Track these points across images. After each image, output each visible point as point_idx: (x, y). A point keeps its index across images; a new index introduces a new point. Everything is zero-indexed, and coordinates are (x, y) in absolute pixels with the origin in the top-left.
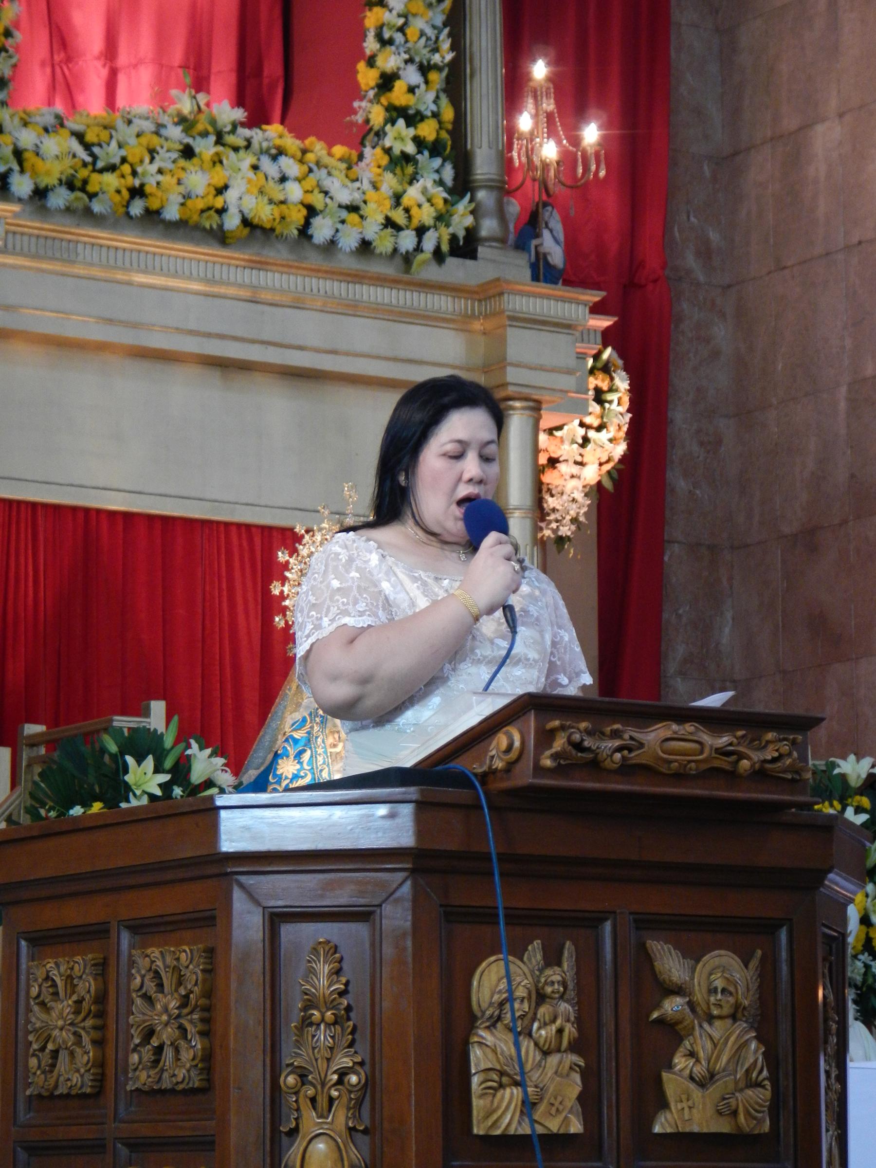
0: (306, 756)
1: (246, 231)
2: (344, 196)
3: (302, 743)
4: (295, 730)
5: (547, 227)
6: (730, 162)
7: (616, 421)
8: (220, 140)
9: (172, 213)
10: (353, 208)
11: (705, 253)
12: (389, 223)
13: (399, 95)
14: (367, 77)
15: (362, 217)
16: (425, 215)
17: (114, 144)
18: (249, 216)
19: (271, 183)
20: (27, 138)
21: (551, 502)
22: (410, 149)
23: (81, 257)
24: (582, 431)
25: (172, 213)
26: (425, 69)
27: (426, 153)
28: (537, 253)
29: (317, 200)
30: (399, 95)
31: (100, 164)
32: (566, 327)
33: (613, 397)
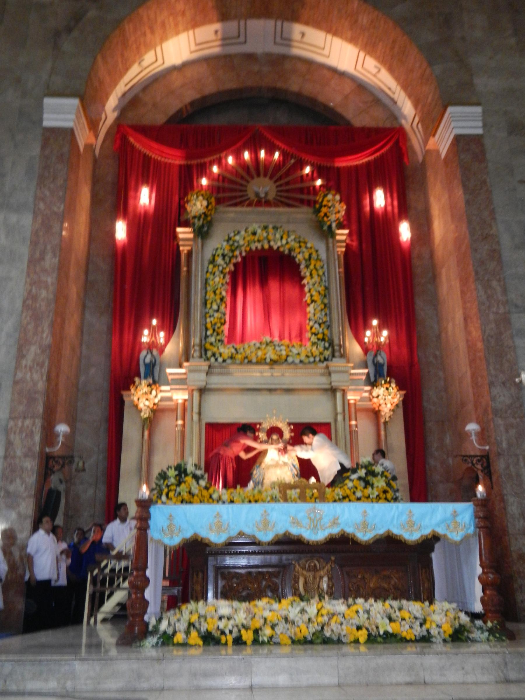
1: (272, 362)
6: (439, 337)
10: (299, 354)
11: (435, 357)
12: (307, 356)
13: (314, 330)
14: (308, 328)
17: (242, 349)
20: (222, 350)
21: (383, 414)
22: (316, 340)
25: (254, 360)
26: (320, 325)
29: (290, 354)
30: (314, 330)
32: (346, 372)
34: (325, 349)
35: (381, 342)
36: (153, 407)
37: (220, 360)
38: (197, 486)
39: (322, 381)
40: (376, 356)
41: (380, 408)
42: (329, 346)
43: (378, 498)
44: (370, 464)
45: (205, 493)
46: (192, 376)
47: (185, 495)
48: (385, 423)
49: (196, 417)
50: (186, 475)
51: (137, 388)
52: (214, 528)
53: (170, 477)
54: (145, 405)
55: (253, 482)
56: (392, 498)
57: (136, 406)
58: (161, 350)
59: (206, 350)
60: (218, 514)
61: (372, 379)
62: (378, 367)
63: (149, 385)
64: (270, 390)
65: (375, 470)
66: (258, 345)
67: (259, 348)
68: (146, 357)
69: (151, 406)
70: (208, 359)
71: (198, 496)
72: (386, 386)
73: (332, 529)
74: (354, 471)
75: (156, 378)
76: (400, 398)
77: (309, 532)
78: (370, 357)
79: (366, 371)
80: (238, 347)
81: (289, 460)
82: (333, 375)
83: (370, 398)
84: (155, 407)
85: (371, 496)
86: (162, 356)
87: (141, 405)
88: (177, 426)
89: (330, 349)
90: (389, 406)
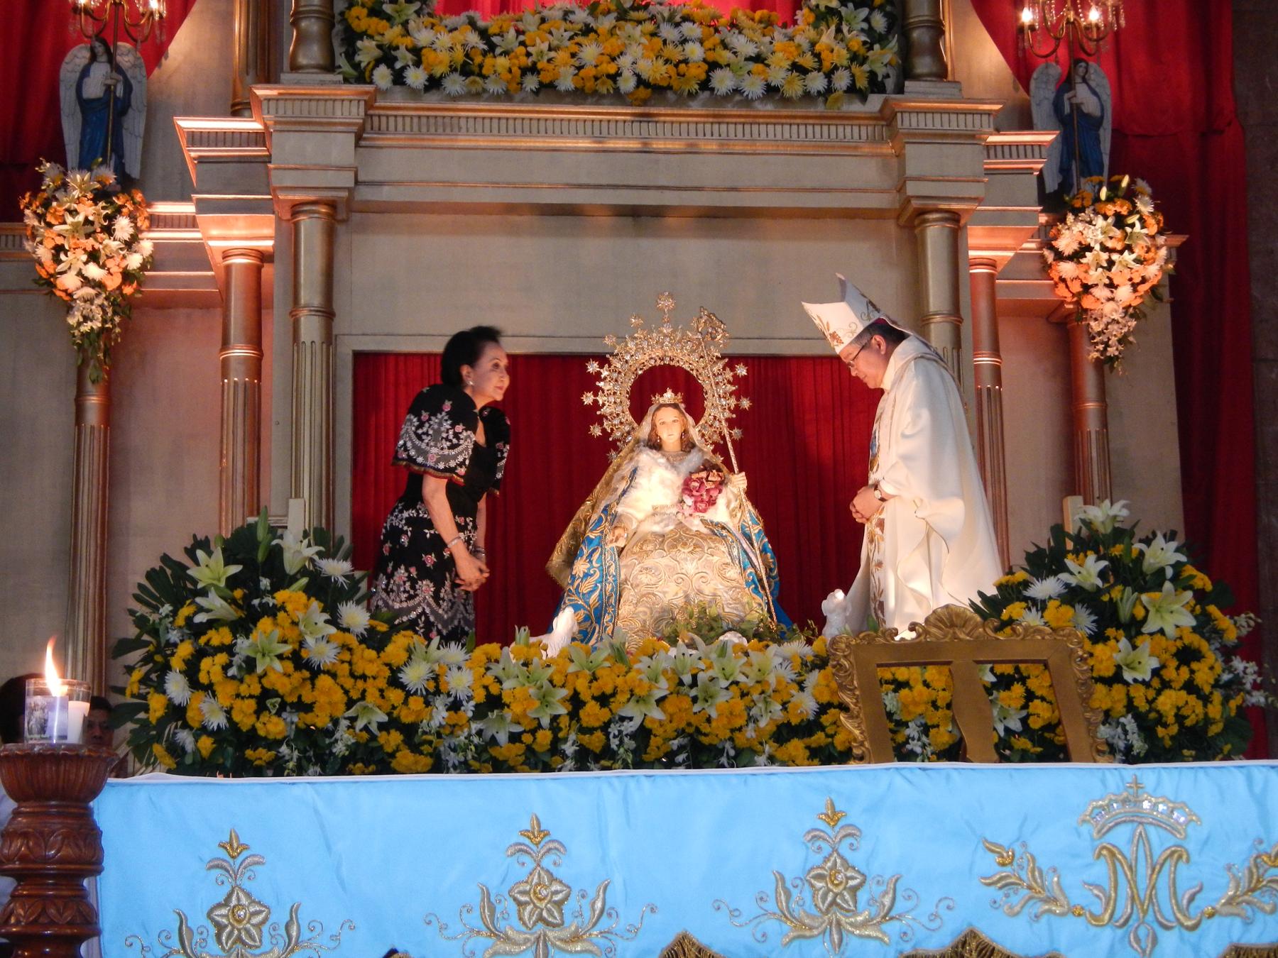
0: (596, 556)
1: (643, 93)
2: (751, 50)
3: (595, 543)
4: (591, 531)
5: (1085, 80)
7: (1142, 243)
8: (622, 16)
9: (567, 82)
10: (758, 59)
15: (768, 66)
16: (841, 55)
17: (512, 32)
18: (645, 76)
19: (670, 47)
20: (423, 37)
21: (1096, 326)
23: (464, 130)
24: (1105, 256)
25: (567, 82)
27: (851, 5)
28: (1071, 105)
29: (725, 56)
31: (498, 51)
32: (972, 137)
33: (1134, 219)
34: (875, 38)
35: (1088, 28)
36: (119, 288)
37: (416, 77)
38: (332, 630)
39: (857, 174)
40: (1067, 83)
41: (1087, 303)
42: (890, 28)
43: (1156, 683)
44: (1120, 534)
45: (368, 661)
46: (287, 148)
47: (278, 674)
48: (1105, 364)
49: (311, 328)
50: (282, 581)
51: (46, 204)
52: (510, 925)
53: (204, 593)
54: (87, 281)
55: (576, 608)
56: (1216, 684)
57: (49, 284)
58: (155, 53)
59: (351, 37)
60: (537, 833)
61: (1051, 185)
62: (1075, 127)
63: (101, 195)
64: (638, 217)
65: (1142, 554)
66: (581, 16)
67: (587, 30)
68: (85, 72)
69: (113, 283)
70: (362, 76)
71: (334, 676)
72: (1111, 209)
73: (1248, 922)
74: (1046, 562)
75: (134, 170)
76: (1167, 261)
77: (1107, 935)
78: (1042, 93)
79: (1049, 138)
80: (492, 23)
81: (732, 515)
82: (910, 150)
83: (1042, 256)
84: (128, 290)
85: (1128, 676)
86: (156, 72)
87: (69, 281)
88: (225, 364)
89: (894, 43)
90: (1124, 293)
